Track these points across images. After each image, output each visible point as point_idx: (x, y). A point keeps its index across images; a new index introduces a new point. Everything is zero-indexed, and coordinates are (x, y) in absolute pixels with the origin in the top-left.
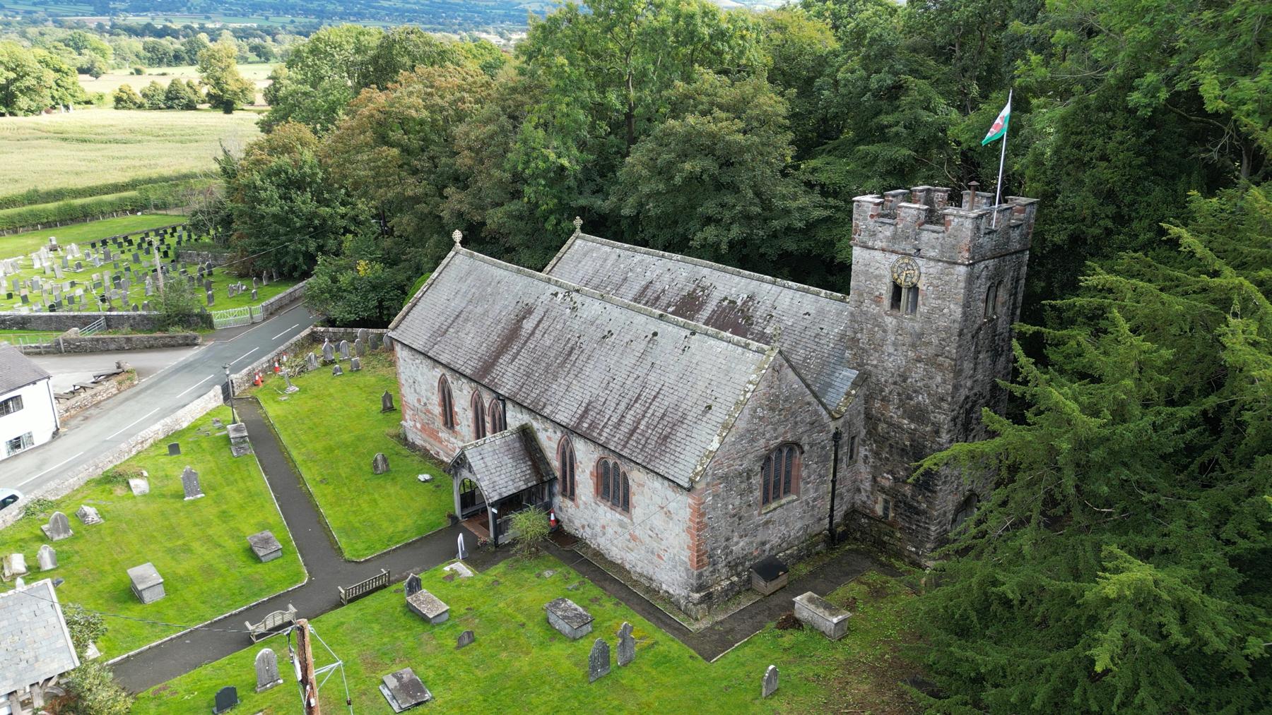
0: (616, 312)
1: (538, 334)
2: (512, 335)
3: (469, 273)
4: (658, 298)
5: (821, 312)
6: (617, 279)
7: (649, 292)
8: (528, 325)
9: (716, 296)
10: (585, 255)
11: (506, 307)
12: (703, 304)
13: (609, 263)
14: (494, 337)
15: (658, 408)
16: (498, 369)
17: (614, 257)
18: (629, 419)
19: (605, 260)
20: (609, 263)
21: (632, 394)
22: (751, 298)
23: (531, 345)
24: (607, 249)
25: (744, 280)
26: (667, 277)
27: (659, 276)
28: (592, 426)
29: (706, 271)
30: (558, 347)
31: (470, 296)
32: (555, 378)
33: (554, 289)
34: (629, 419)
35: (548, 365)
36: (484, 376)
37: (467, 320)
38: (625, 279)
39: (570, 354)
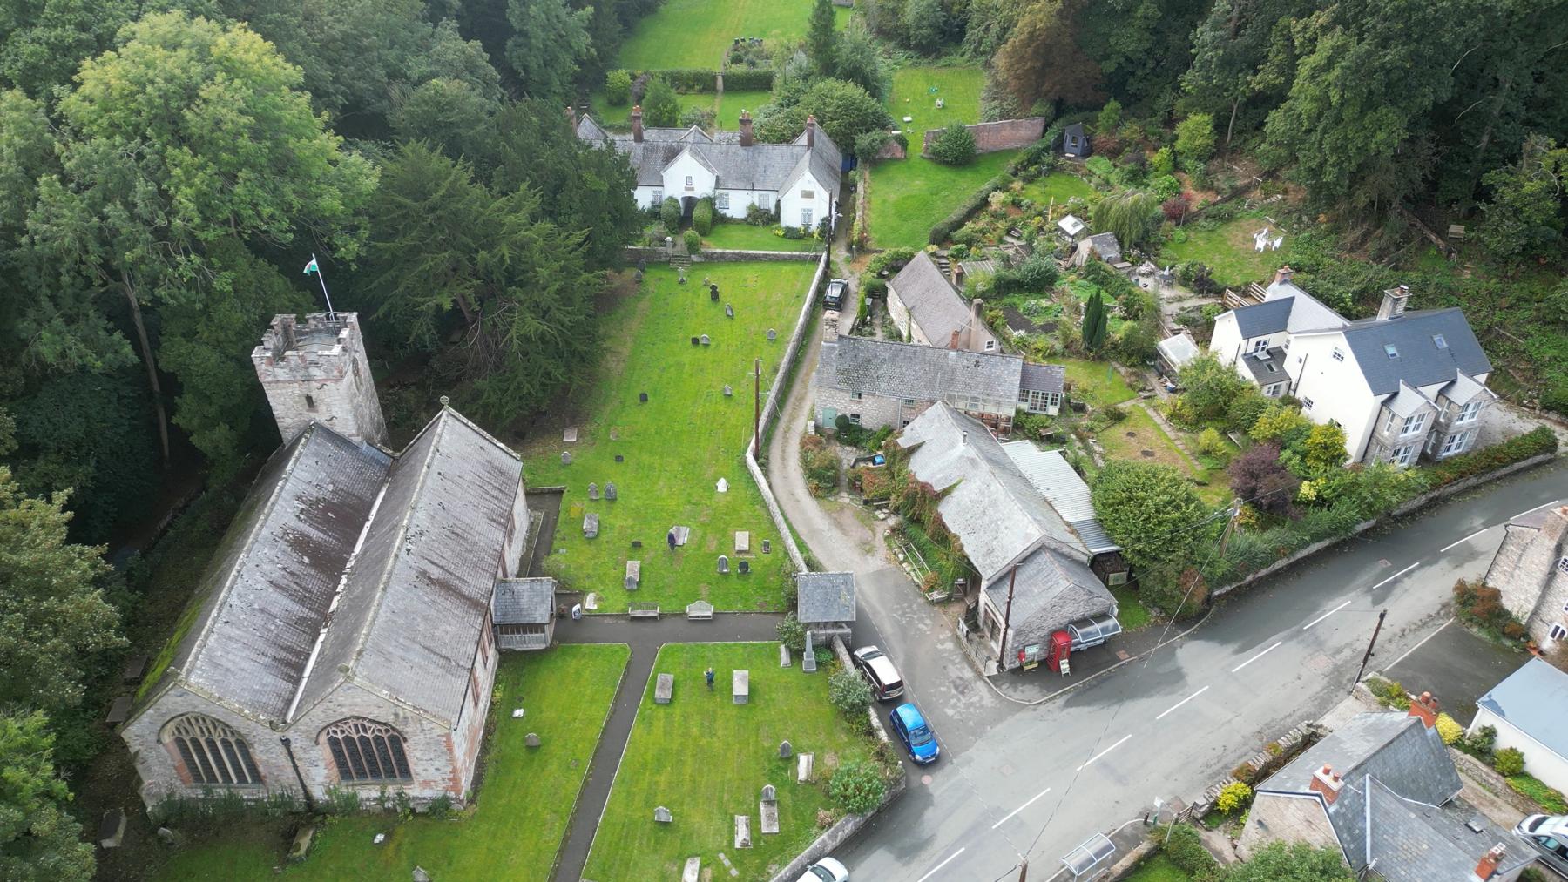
0: (425, 500)
1: (443, 563)
2: (445, 587)
3: (381, 652)
4: (292, 574)
5: (316, 454)
6: (259, 620)
7: (284, 582)
8: (436, 573)
9: (293, 523)
10: (217, 666)
11: (419, 597)
12: (302, 534)
13: (234, 632)
14: (448, 604)
15: (484, 475)
16: (475, 595)
17: (227, 629)
18: (495, 493)
19: (230, 638)
20: (234, 632)
21: (480, 491)
22: (299, 498)
23: (451, 568)
24: (212, 640)
25: (280, 502)
26: (267, 567)
27: (264, 574)
28: (501, 516)
29: (265, 532)
30: (453, 545)
31: (408, 643)
32: (475, 544)
33: (403, 553)
34: (495, 493)
35: (467, 551)
36: (482, 605)
37: (433, 637)
38: (262, 610)
39: (456, 535)
